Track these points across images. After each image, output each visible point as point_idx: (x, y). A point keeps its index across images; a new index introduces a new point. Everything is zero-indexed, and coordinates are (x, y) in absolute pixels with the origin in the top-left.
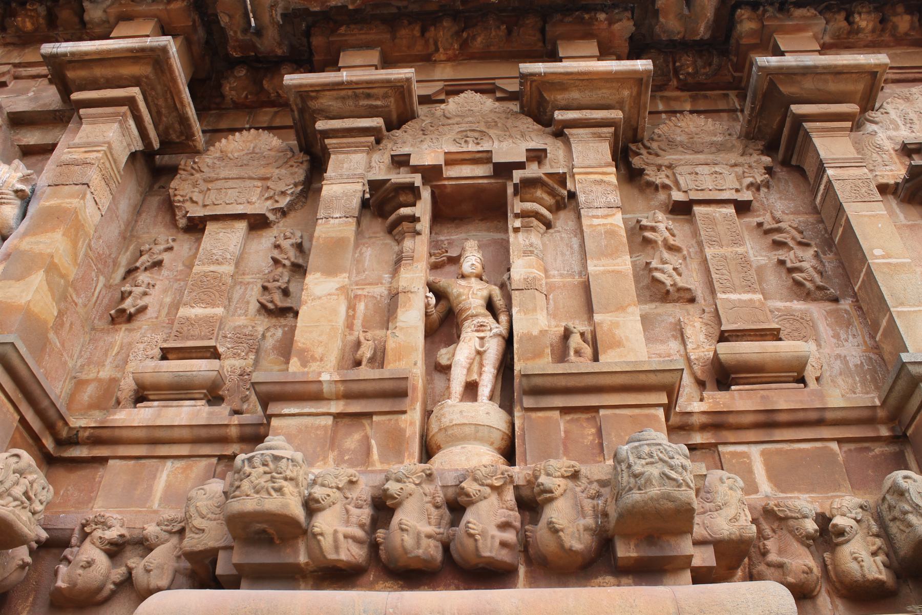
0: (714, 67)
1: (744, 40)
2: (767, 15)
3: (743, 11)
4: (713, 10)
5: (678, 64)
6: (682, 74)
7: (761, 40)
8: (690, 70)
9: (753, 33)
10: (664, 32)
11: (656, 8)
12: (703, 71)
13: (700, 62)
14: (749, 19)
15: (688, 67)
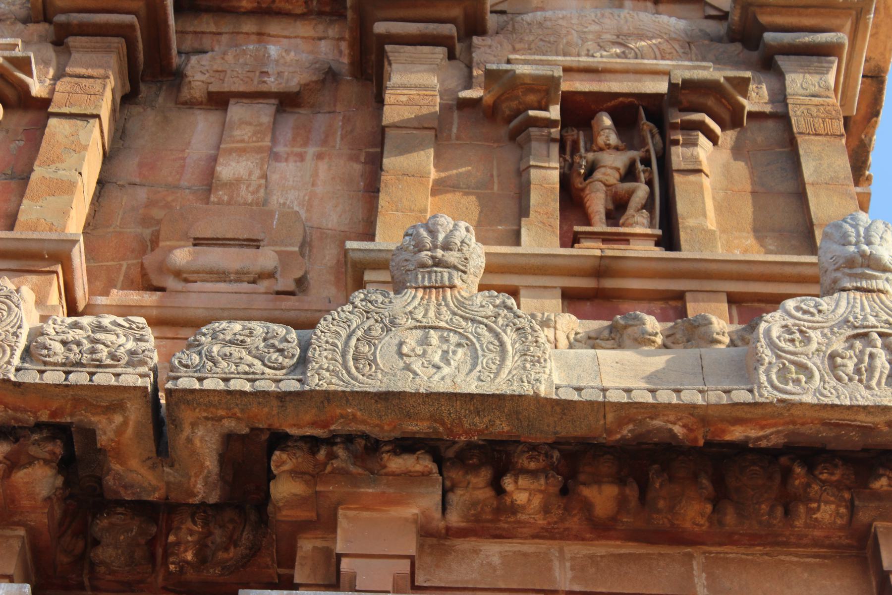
0: (242, 550)
1: (284, 513)
2: (336, 463)
3: (284, 456)
4: (215, 457)
5: (172, 538)
6: (173, 563)
7: (318, 515)
8: (189, 556)
9: (301, 502)
10: (125, 487)
11: (99, 446)
12: (221, 555)
13: (218, 536)
14: (295, 473)
15: (186, 551)
